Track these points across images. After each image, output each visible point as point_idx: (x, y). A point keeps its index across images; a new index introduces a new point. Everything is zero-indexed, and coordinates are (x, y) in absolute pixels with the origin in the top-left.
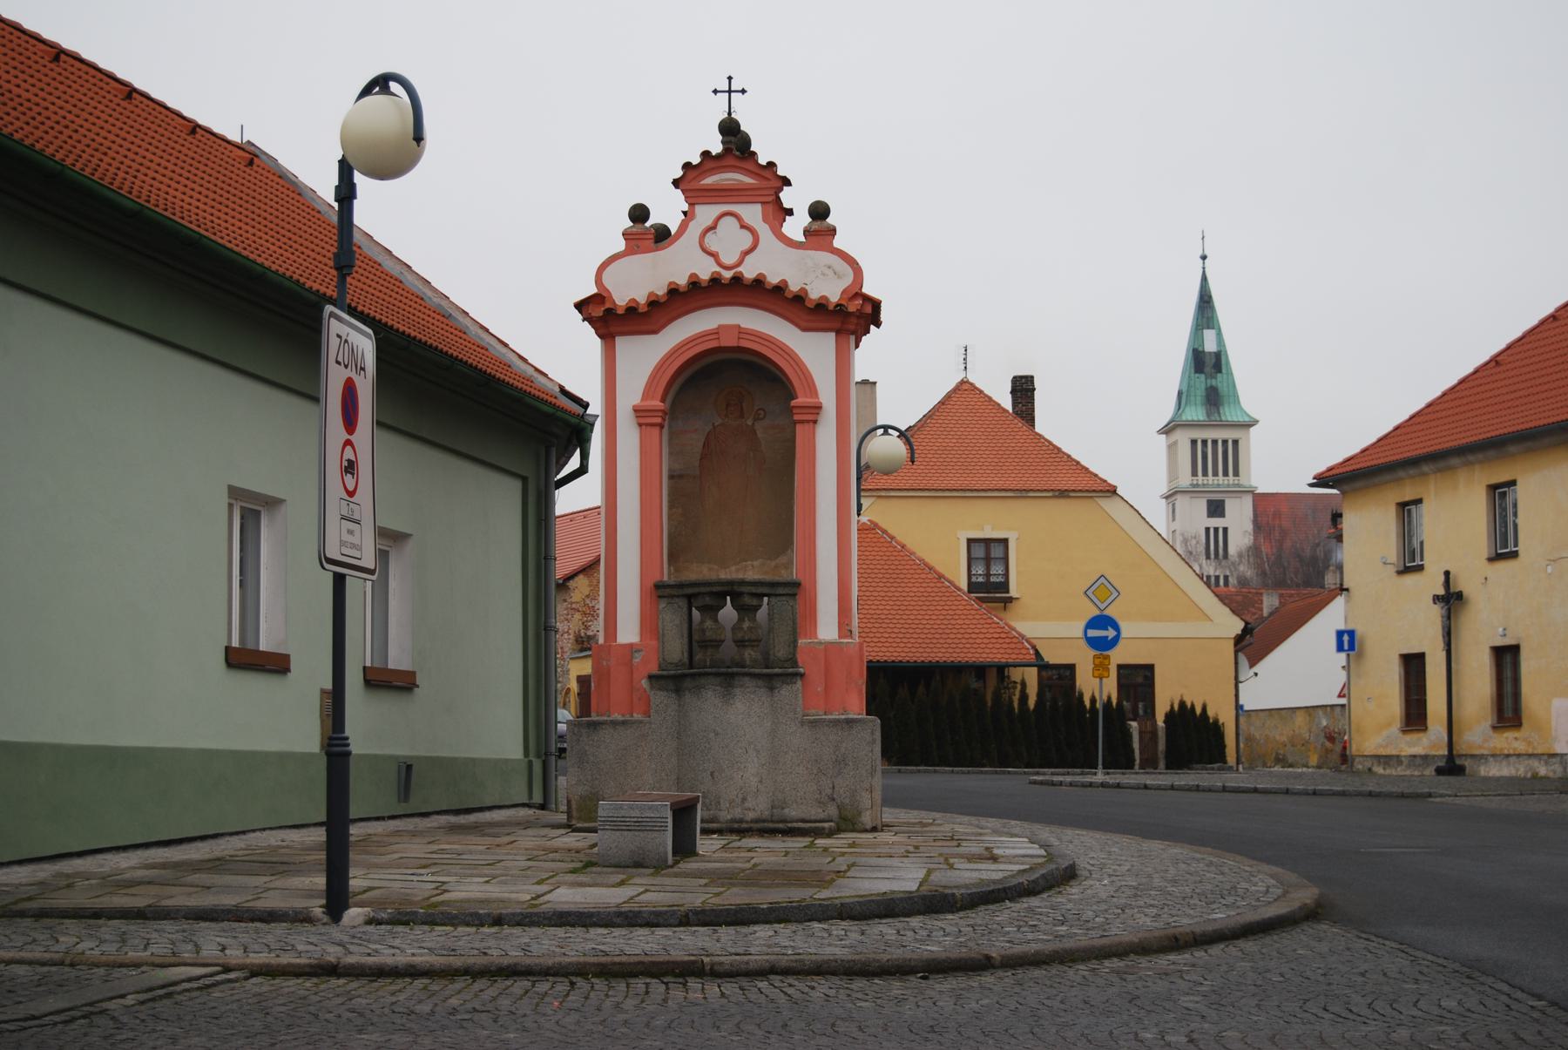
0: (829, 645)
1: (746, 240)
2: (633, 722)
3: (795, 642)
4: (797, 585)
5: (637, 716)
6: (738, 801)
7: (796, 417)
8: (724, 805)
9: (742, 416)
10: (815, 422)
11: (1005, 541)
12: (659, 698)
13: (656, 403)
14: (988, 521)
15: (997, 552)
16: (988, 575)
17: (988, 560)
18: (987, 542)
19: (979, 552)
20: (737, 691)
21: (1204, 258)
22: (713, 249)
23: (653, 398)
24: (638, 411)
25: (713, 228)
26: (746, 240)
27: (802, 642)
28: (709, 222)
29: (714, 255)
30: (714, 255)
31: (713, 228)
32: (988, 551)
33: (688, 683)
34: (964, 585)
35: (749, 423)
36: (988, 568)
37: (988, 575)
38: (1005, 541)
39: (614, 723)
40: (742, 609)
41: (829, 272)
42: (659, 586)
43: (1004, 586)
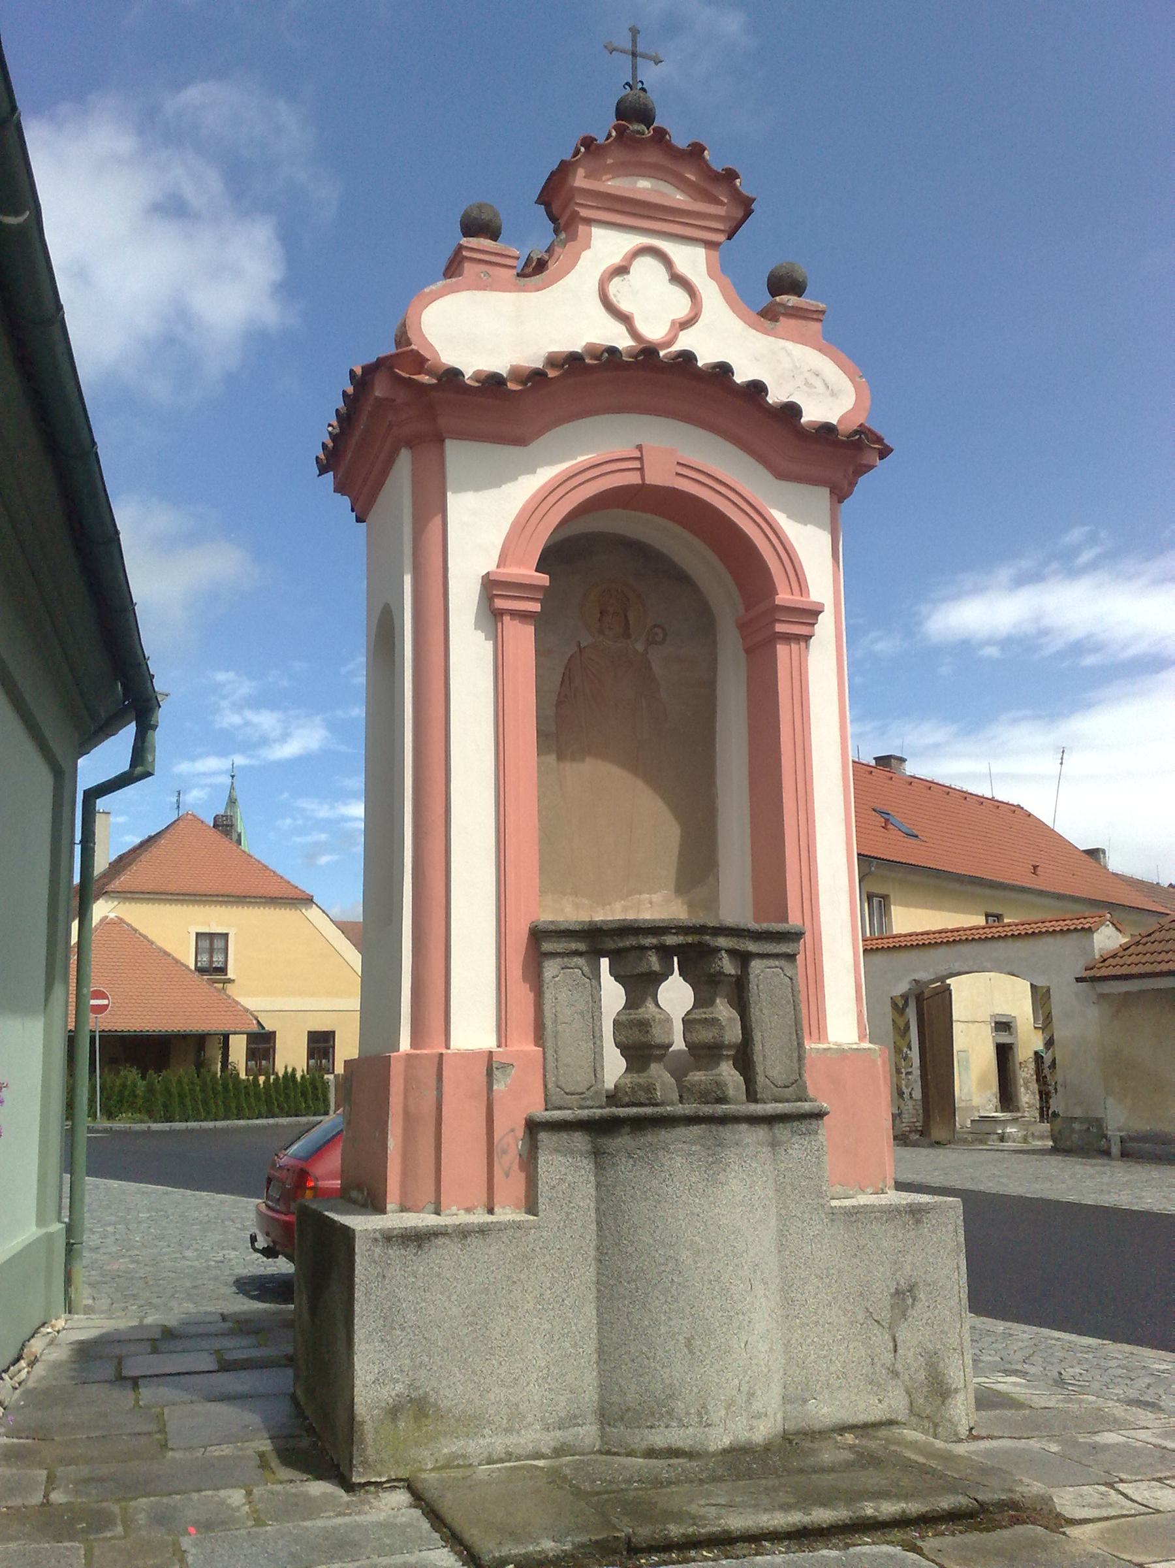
0: (843, 1054)
1: (680, 305)
2: (502, 1227)
3: (800, 1045)
4: (797, 936)
5: (506, 1214)
6: (741, 1400)
7: (780, 628)
8: (717, 1413)
9: (627, 634)
10: (807, 638)
11: (225, 936)
12: (565, 1169)
13: (527, 571)
14: (214, 919)
15: (219, 944)
16: (211, 962)
17: (211, 951)
18: (211, 936)
19: (205, 944)
20: (730, 1155)
21: (233, 777)
22: (624, 306)
23: (520, 563)
24: (491, 586)
25: (622, 270)
26: (680, 305)
27: (809, 1045)
28: (616, 260)
29: (625, 319)
30: (625, 319)
31: (622, 270)
32: (212, 942)
33: (623, 1141)
34: (193, 968)
35: (640, 647)
36: (212, 957)
37: (211, 962)
38: (225, 936)
39: (464, 1233)
40: (706, 985)
41: (818, 383)
42: (537, 934)
43: (223, 970)
